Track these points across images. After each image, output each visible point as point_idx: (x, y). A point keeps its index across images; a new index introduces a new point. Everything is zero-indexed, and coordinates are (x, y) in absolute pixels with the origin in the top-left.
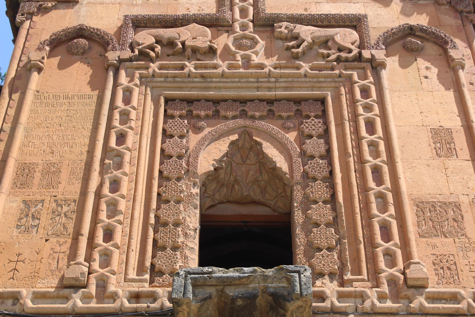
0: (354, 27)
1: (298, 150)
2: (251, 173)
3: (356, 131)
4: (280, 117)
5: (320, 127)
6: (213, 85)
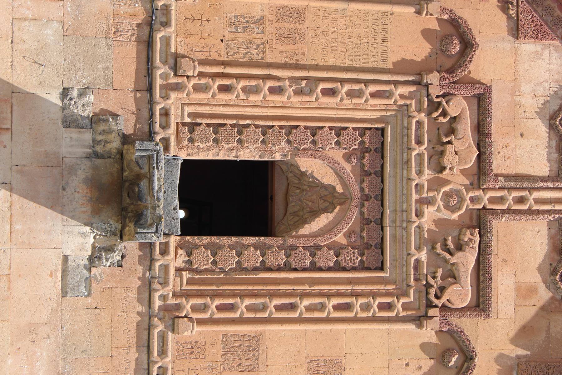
0: (478, 306)
1: (322, 244)
2: (310, 204)
3: (339, 294)
4: (362, 230)
5: (348, 264)
6: (399, 171)
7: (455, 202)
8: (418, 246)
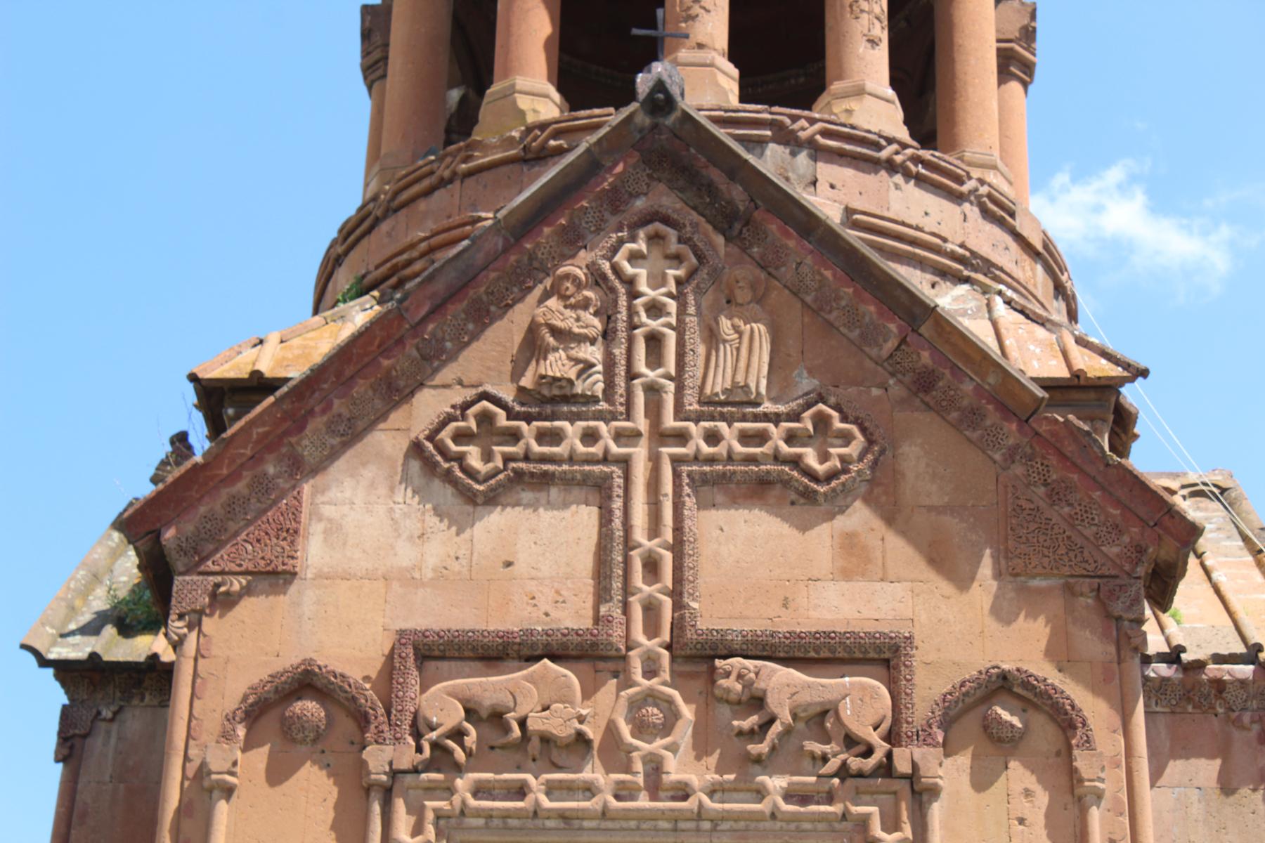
7: (656, 711)
8: (754, 795)
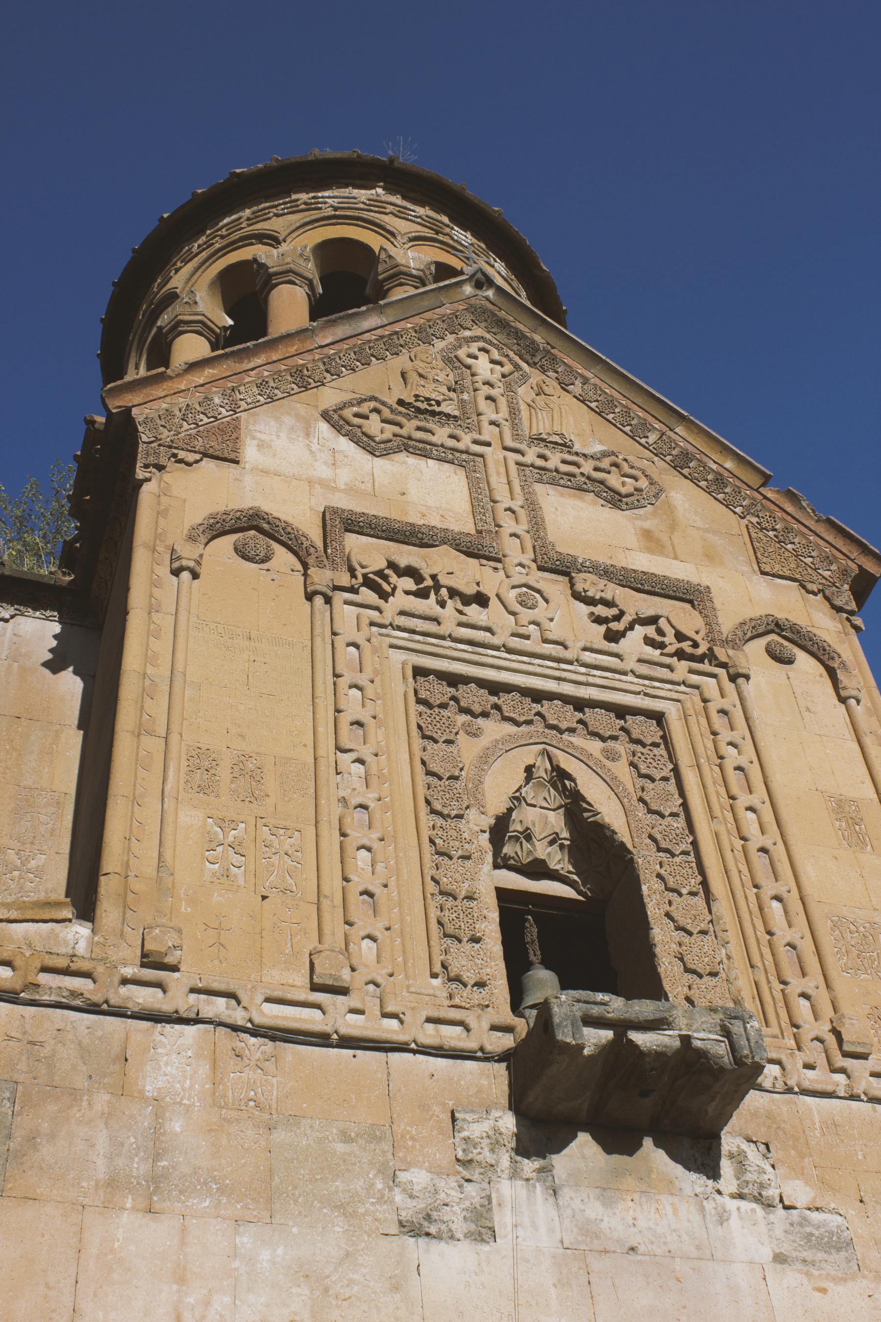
0: (690, 602)
